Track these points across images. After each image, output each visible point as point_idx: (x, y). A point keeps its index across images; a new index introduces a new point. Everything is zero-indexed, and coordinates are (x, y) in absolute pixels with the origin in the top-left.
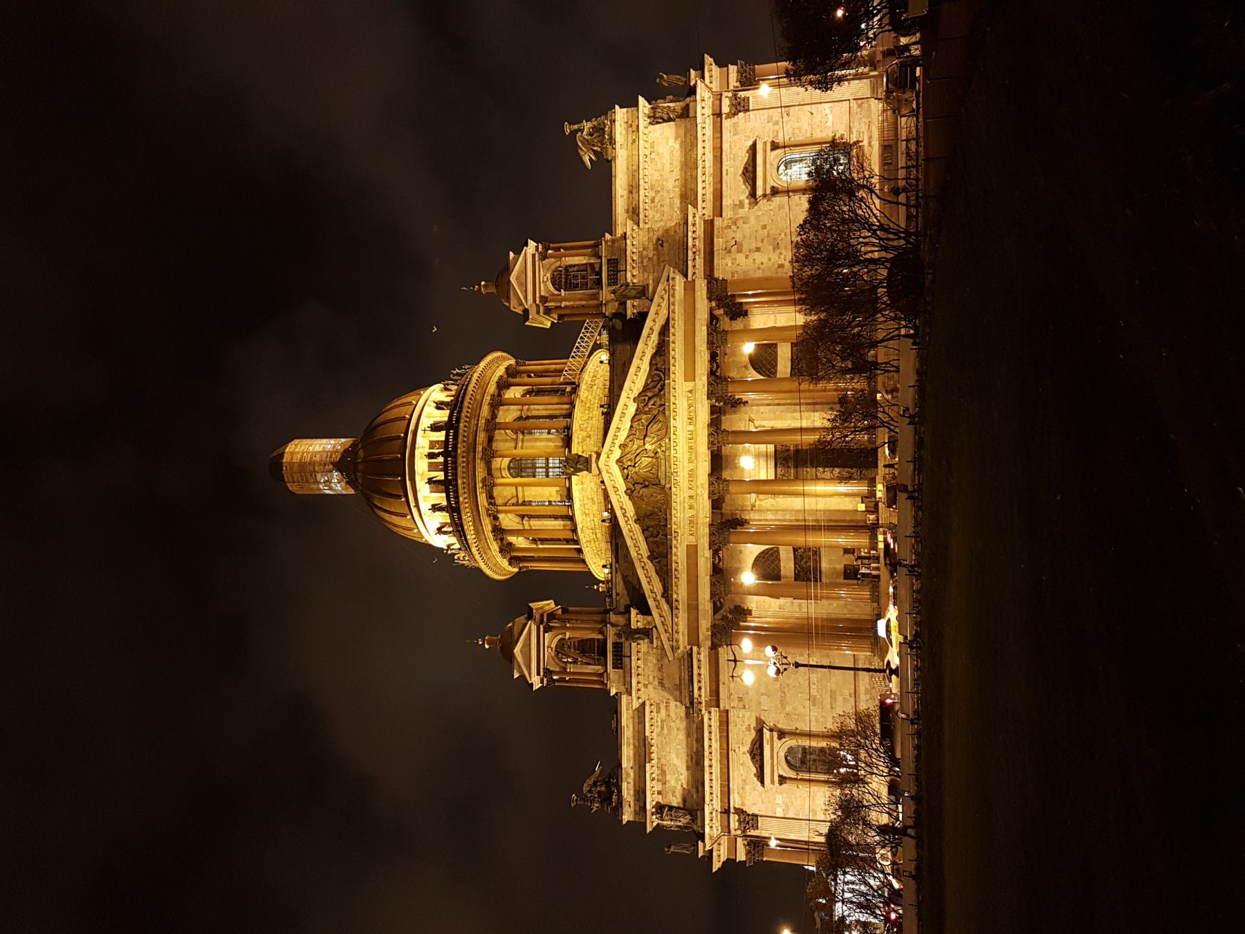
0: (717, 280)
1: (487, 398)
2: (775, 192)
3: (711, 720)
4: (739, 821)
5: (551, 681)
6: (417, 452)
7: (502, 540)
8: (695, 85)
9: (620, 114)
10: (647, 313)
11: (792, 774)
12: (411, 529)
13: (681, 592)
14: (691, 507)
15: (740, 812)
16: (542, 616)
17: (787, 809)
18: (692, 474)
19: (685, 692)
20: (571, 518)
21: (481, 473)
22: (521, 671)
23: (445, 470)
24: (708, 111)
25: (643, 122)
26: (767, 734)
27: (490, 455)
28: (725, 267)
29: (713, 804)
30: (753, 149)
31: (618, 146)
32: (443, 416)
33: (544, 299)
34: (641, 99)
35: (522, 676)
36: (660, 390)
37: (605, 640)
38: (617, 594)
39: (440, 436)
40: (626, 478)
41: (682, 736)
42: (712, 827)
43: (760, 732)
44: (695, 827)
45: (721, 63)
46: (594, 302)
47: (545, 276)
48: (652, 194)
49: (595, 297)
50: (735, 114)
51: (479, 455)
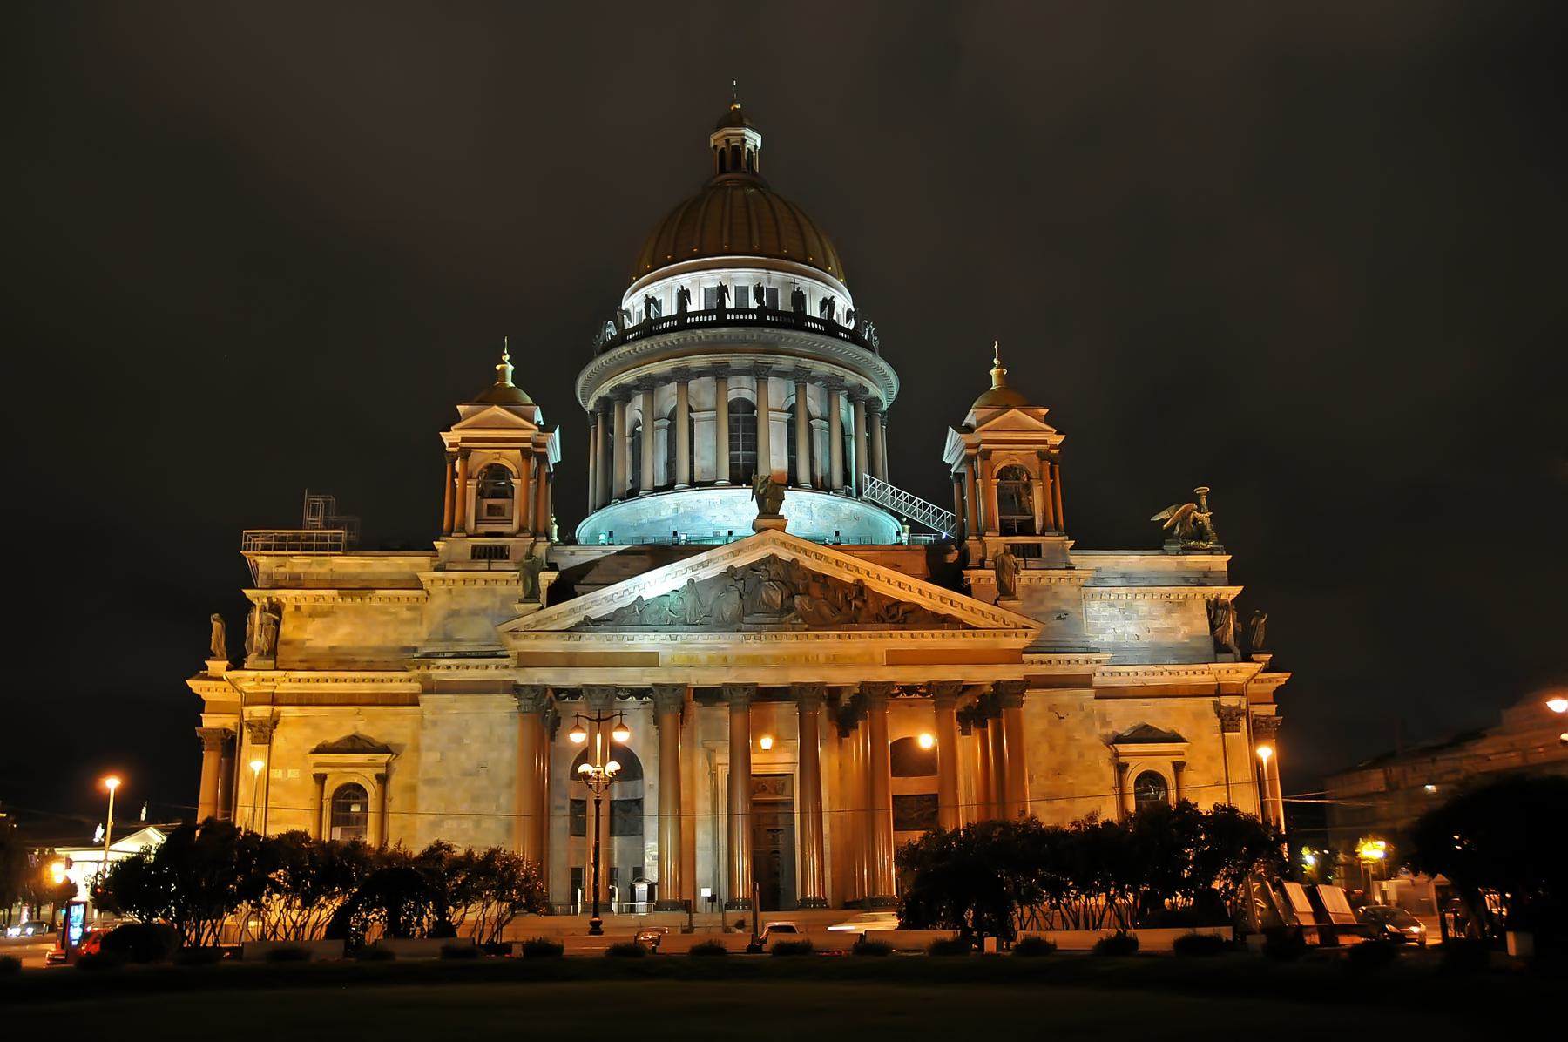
0: (1022, 694)
3: (399, 683)
7: (637, 388)
8: (1251, 661)
9: (1220, 562)
13: (593, 642)
15: (275, 722)
16: (544, 445)
17: (278, 782)
20: (669, 487)
21: (736, 360)
22: (468, 415)
24: (1225, 679)
25: (1212, 591)
29: (285, 682)
30: (1177, 739)
31: (1181, 558)
32: (813, 310)
33: (986, 455)
34: (1240, 589)
35: (457, 418)
38: (573, 553)
39: (784, 303)
41: (375, 640)
43: (385, 749)
45: (1279, 695)
47: (1018, 457)
50: (1218, 714)
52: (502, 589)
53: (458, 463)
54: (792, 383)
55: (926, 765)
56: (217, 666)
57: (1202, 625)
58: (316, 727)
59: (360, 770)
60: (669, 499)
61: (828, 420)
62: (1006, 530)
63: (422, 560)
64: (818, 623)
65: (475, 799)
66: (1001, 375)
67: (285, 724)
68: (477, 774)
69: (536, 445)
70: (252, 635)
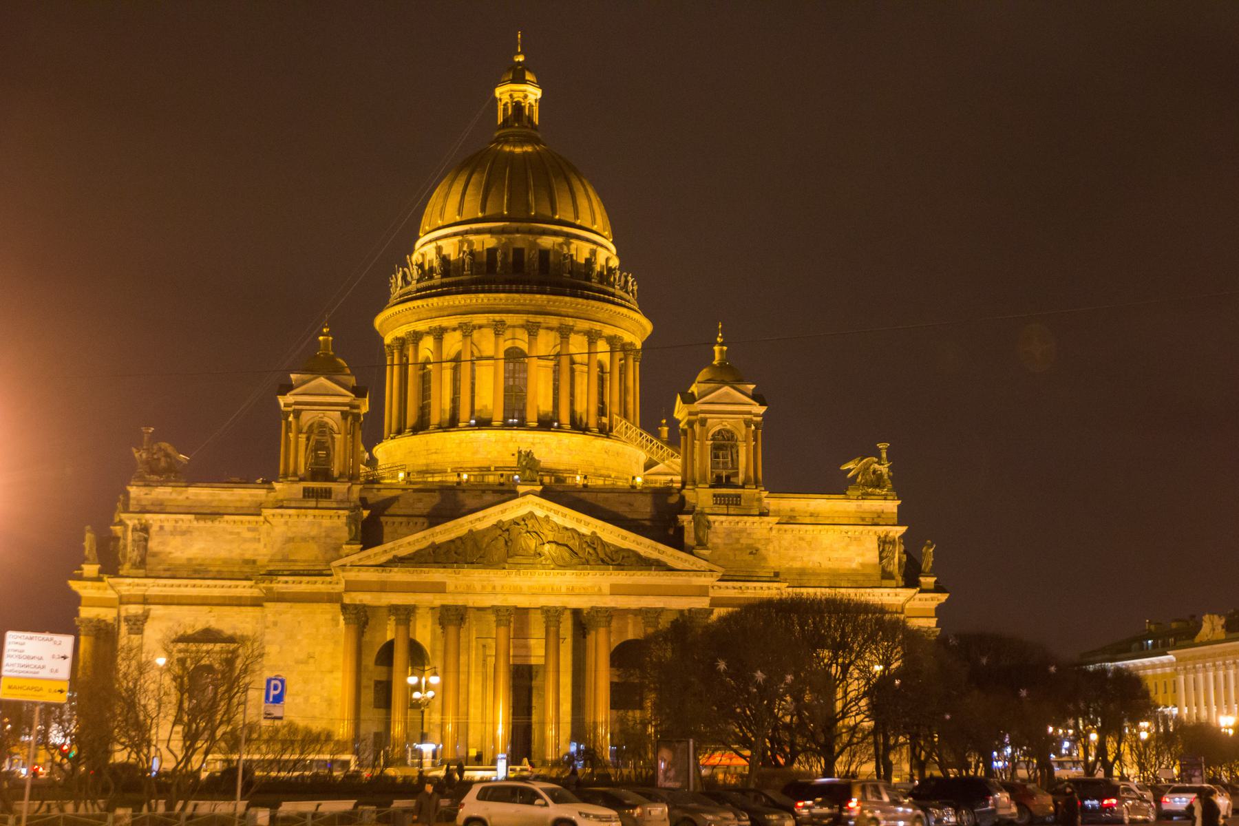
3: (244, 589)
5: (287, 414)
12: (442, 215)
13: (398, 575)
14: (483, 587)
15: (146, 616)
18: (518, 591)
19: (280, 566)
20: (452, 423)
21: (510, 319)
25: (881, 530)
26: (232, 646)
29: (154, 587)
31: (861, 502)
33: (703, 422)
36: (603, 561)
37: (334, 480)
38: (379, 490)
44: (127, 566)
45: (940, 611)
47: (728, 423)
49: (704, 480)
52: (327, 523)
53: (290, 419)
54: (558, 335)
56: (91, 569)
57: (872, 556)
59: (212, 653)
61: (588, 365)
62: (718, 482)
65: (306, 682)
66: (721, 352)
67: (154, 619)
68: (305, 662)
69: (352, 406)
70: (125, 546)
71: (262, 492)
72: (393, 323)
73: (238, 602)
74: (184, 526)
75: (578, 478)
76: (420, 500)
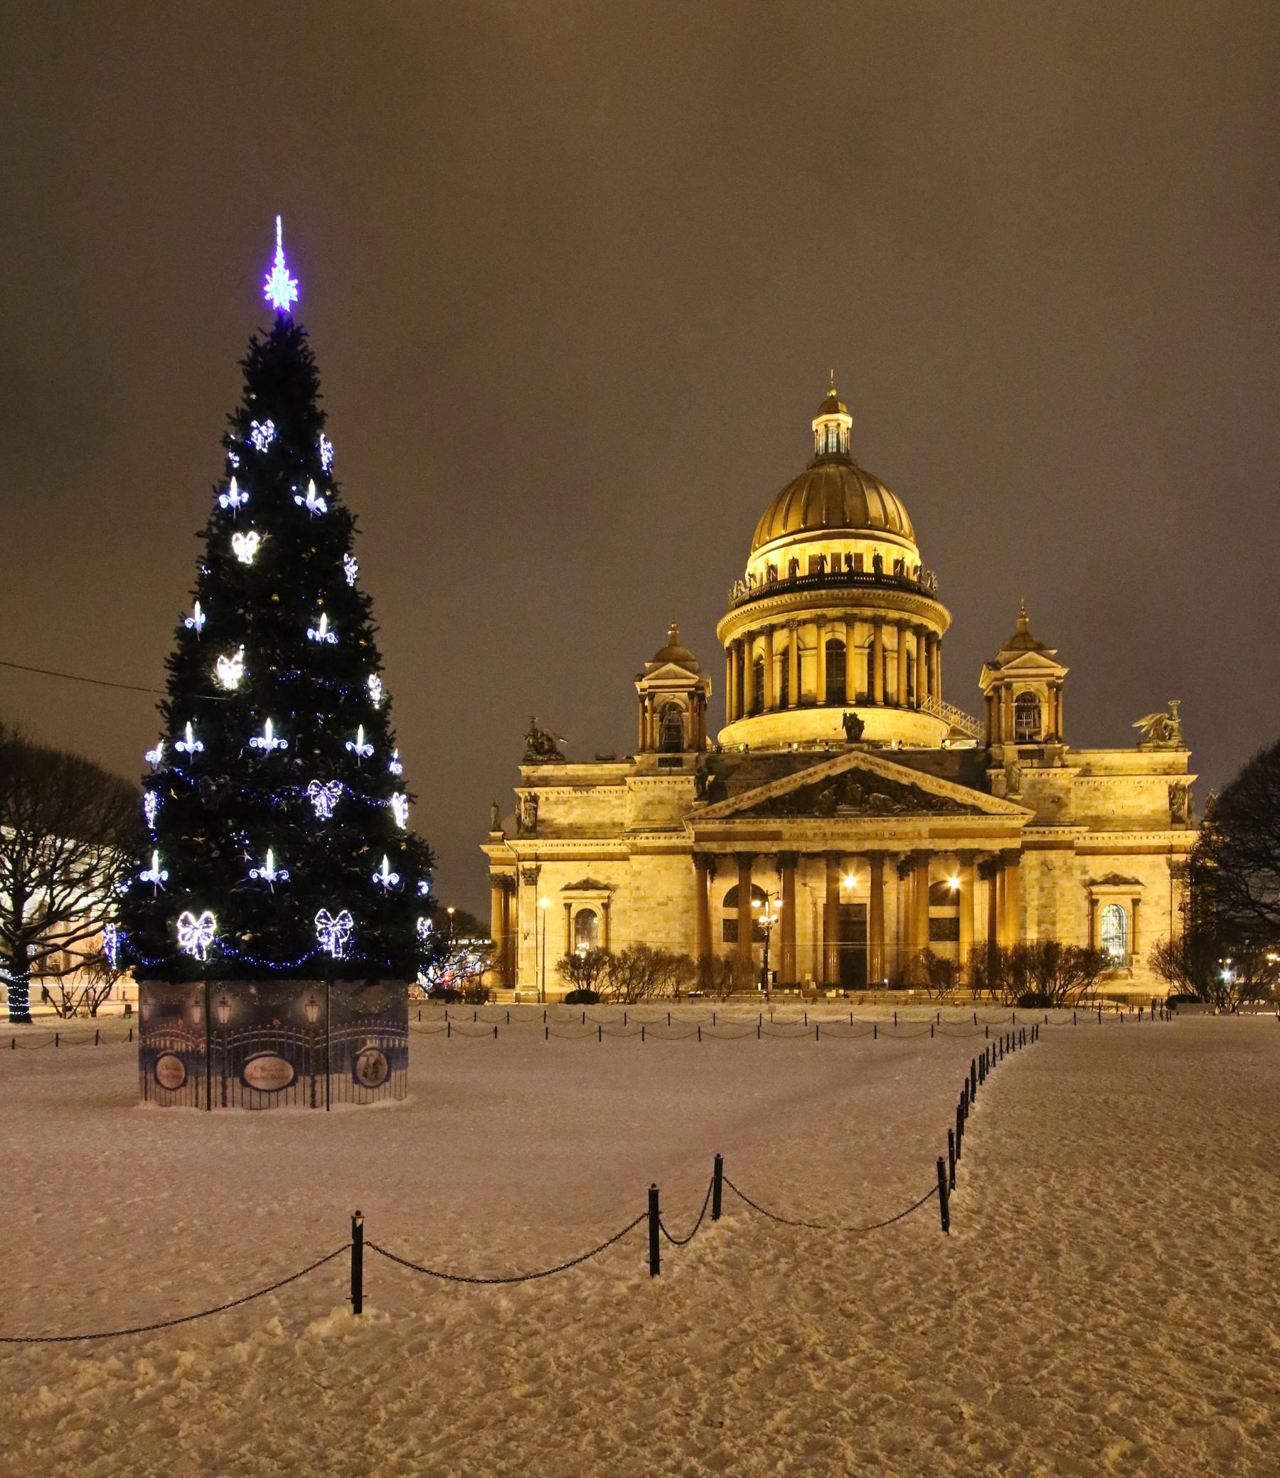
1: (906, 616)
2: (1093, 903)
4: (530, 870)
6: (852, 541)
9: (1183, 757)
10: (988, 791)
11: (573, 914)
12: (769, 533)
13: (740, 826)
15: (538, 869)
16: (702, 688)
20: (783, 706)
21: (831, 612)
23: (833, 574)
24: (1176, 842)
25: (1173, 779)
26: (606, 893)
27: (849, 621)
28: (1031, 859)
31: (1153, 754)
32: (888, 569)
34: (1193, 778)
37: (684, 751)
39: (868, 568)
40: (843, 775)
42: (525, 846)
43: (606, 888)
46: (1003, 736)
48: (1102, 789)
49: (1009, 738)
51: (850, 610)
52: (679, 787)
53: (647, 703)
55: (956, 900)
58: (563, 874)
59: (592, 901)
60: (784, 716)
62: (1021, 739)
63: (626, 767)
64: (881, 810)
71: (627, 766)
72: (733, 626)
73: (611, 857)
74: (565, 796)
75: (893, 744)
76: (757, 767)
